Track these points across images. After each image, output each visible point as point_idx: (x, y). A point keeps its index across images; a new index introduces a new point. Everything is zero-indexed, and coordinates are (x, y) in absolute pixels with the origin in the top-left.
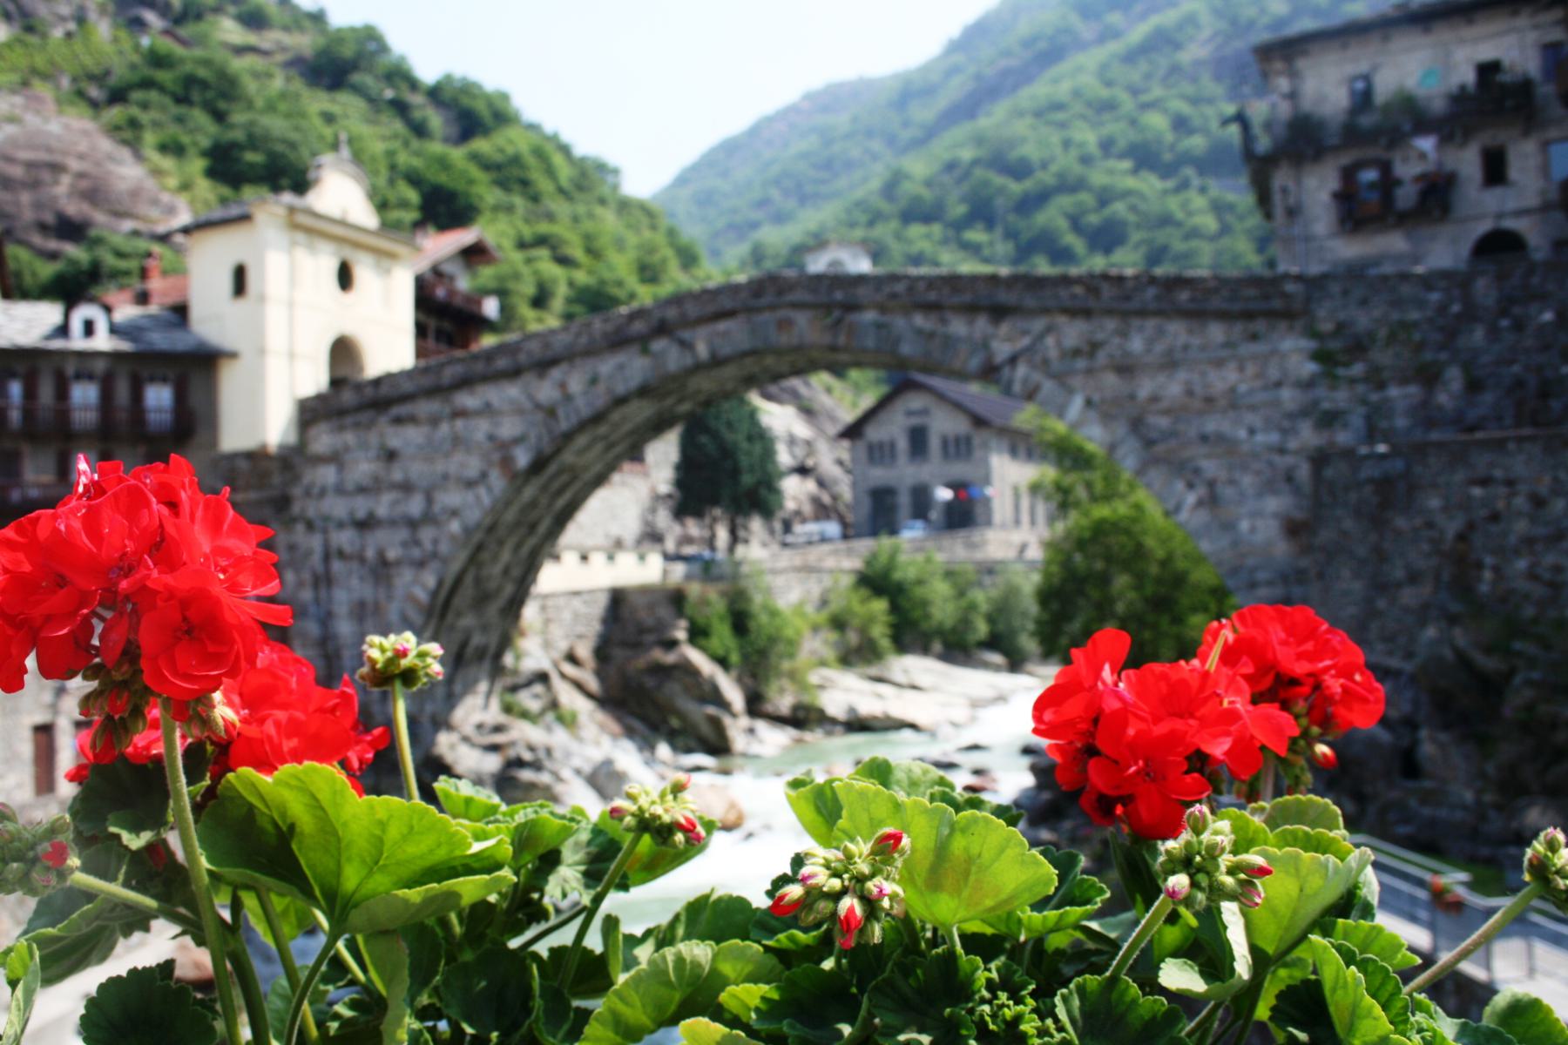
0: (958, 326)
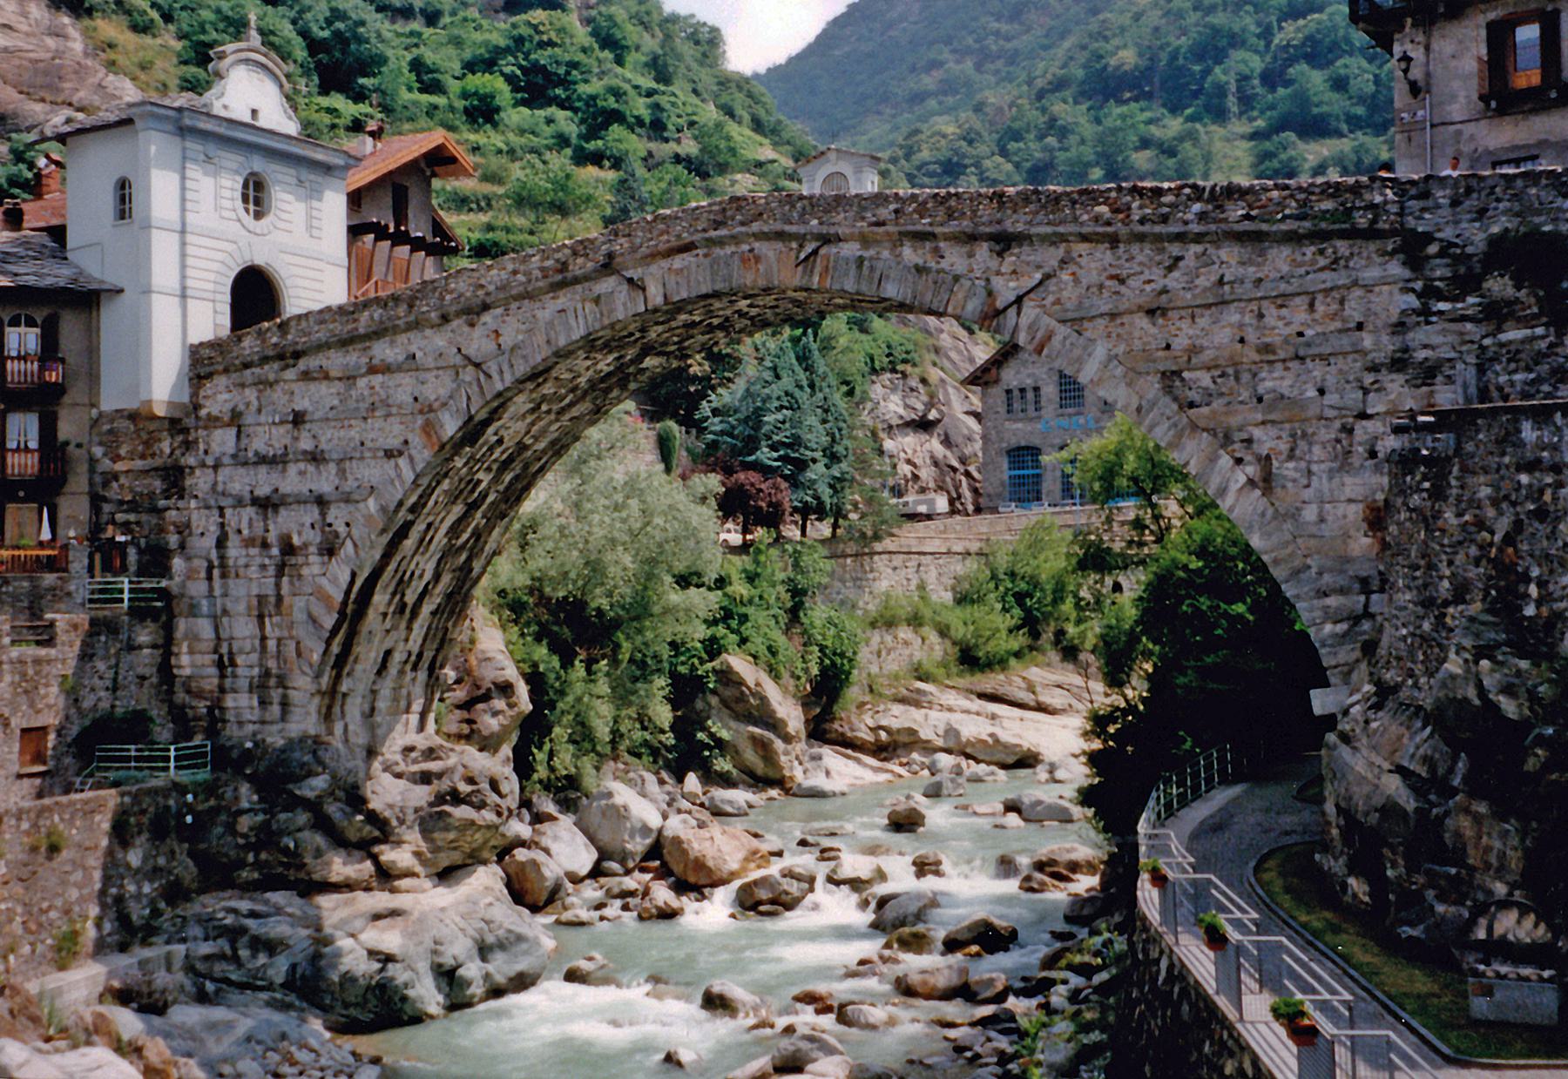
0: (954, 259)
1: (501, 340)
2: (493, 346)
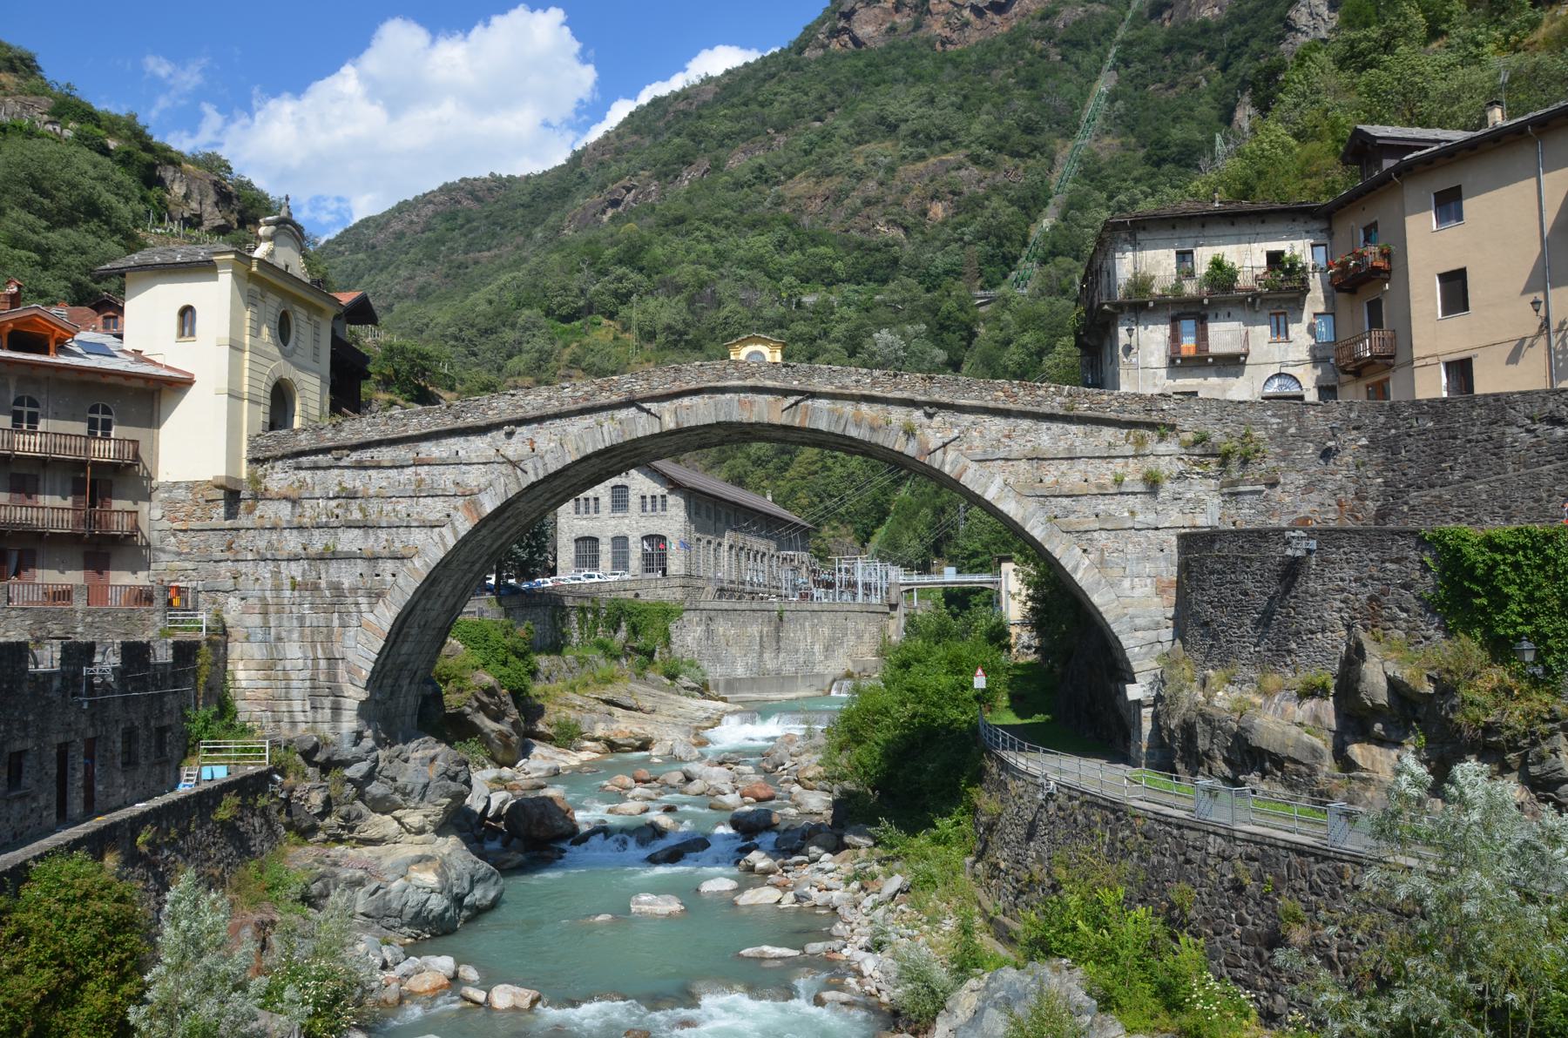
2: (528, 448)
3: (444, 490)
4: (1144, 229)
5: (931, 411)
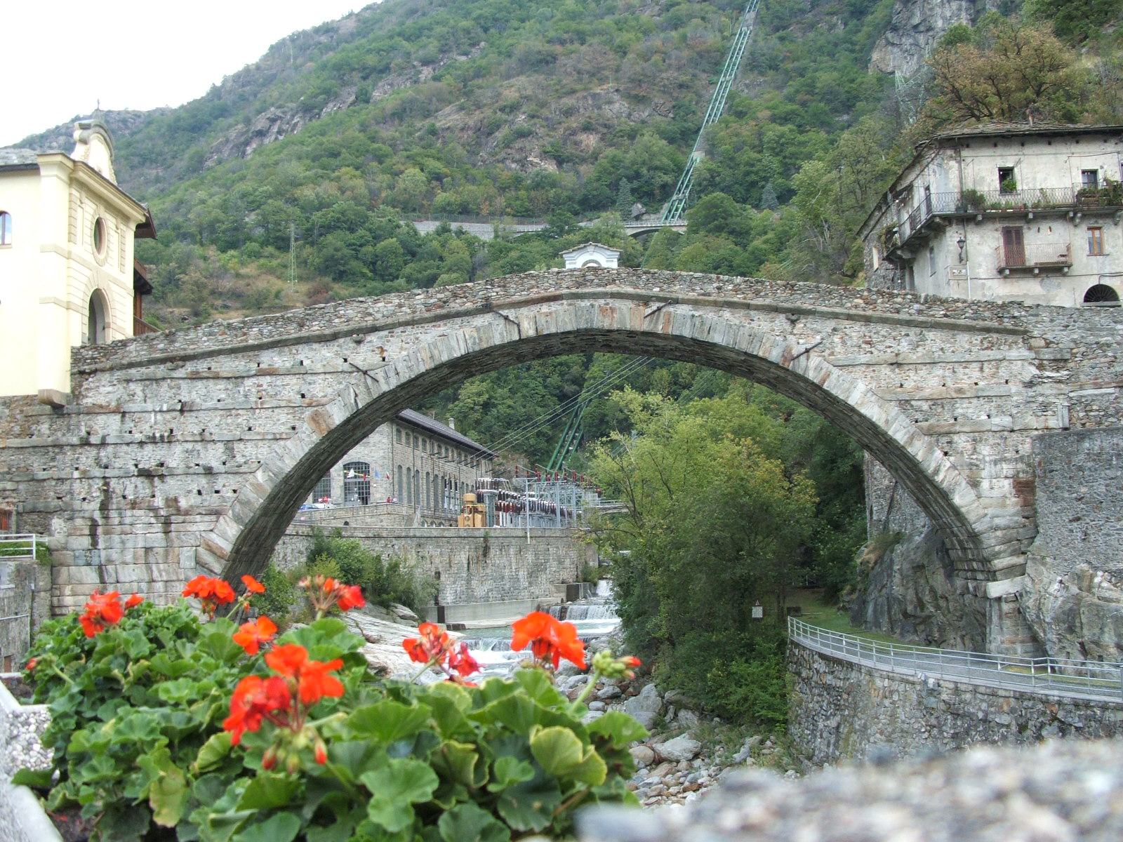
1: (385, 354)
2: (378, 358)
3: (290, 401)
4: (968, 146)
5: (794, 318)
